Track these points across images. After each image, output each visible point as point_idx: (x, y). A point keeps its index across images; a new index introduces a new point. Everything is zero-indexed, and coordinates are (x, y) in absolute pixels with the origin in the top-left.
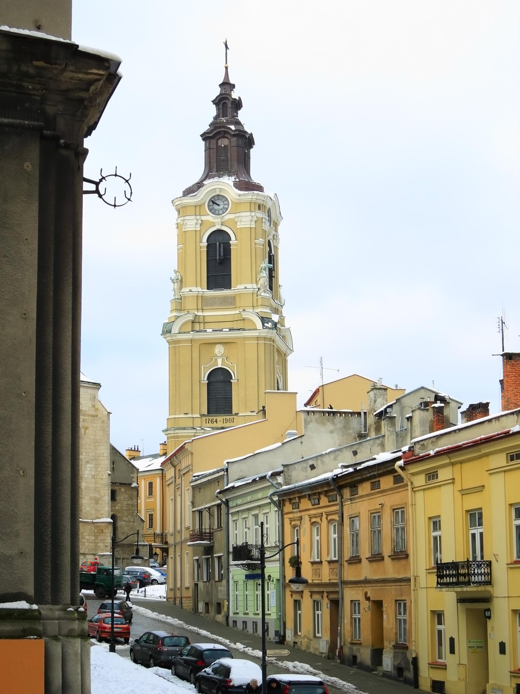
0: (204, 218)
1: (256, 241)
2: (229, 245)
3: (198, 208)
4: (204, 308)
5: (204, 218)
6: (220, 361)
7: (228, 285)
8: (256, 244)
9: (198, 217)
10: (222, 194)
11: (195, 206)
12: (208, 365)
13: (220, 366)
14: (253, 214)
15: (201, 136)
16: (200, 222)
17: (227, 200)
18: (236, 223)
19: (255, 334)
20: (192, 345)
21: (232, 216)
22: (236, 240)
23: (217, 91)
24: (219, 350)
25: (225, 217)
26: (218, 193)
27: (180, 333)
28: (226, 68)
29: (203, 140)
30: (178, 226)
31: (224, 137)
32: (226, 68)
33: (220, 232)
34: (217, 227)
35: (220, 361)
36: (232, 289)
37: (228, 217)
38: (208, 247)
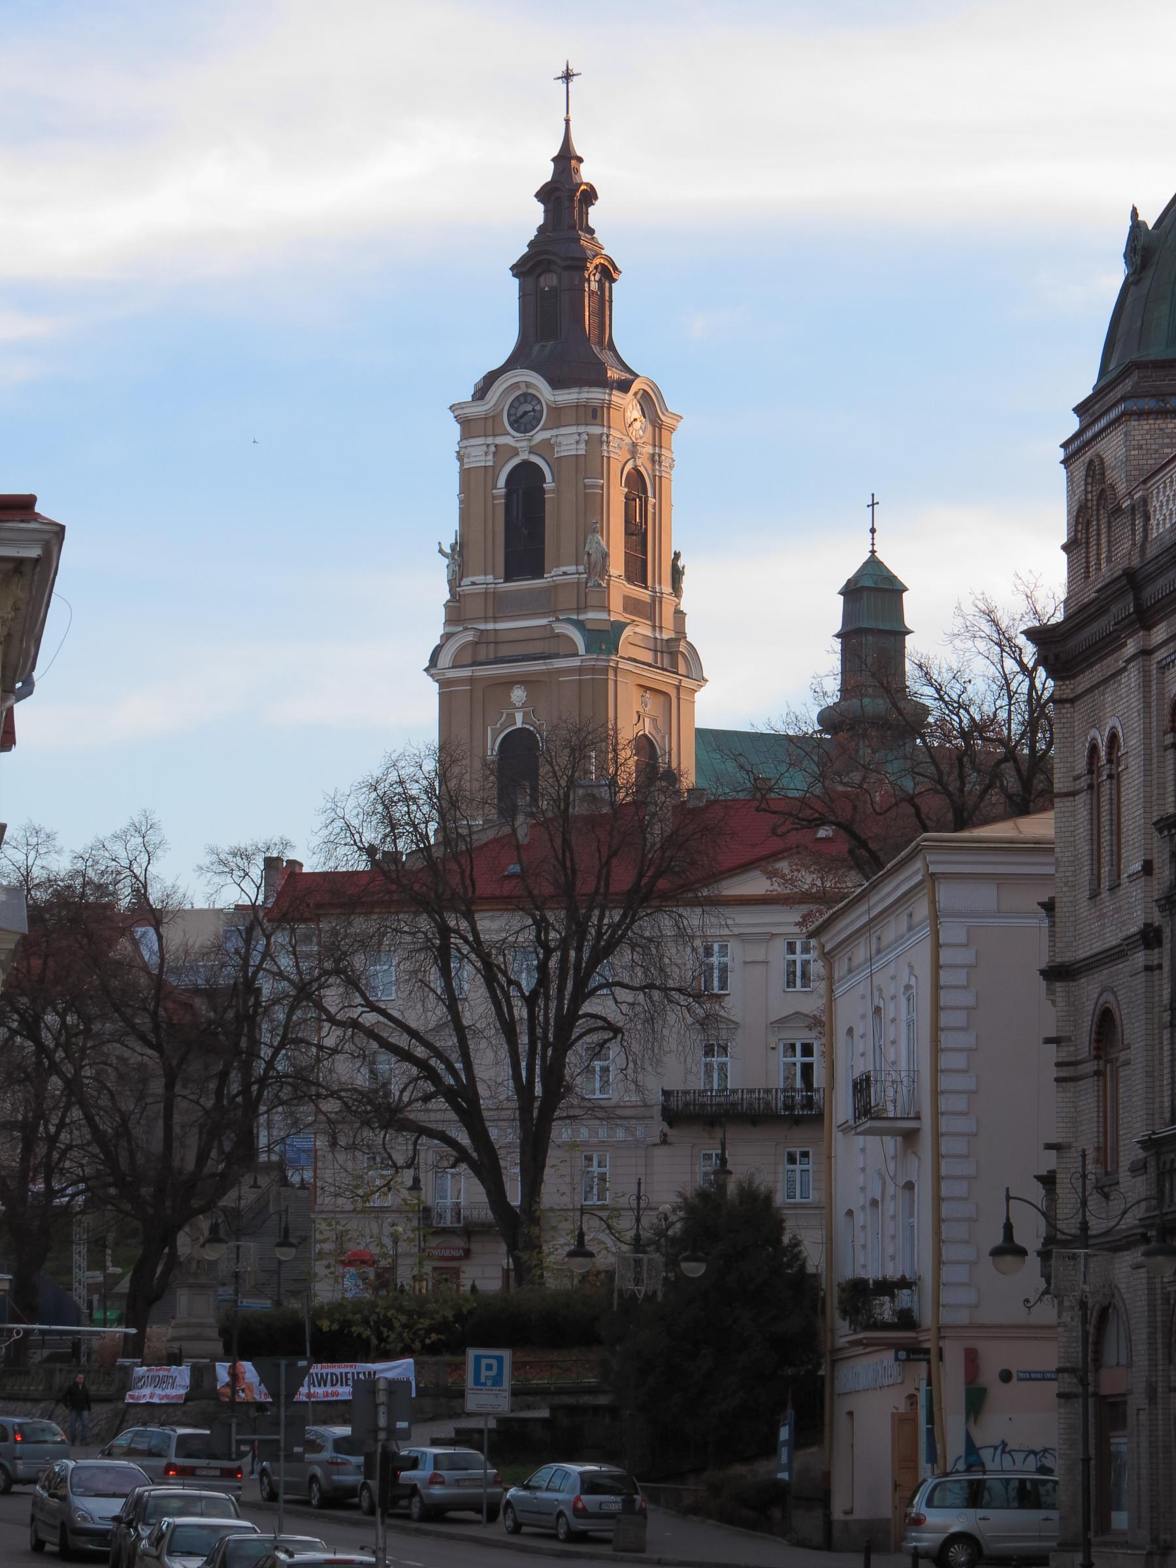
0: (501, 440)
1: (586, 480)
2: (543, 491)
3: (490, 423)
4: (497, 615)
5: (501, 440)
6: (519, 717)
7: (538, 573)
8: (586, 487)
9: (490, 440)
10: (531, 391)
11: (485, 418)
12: (498, 725)
13: (519, 725)
14: (582, 429)
15: (512, 269)
16: (492, 449)
17: (539, 402)
18: (552, 447)
19: (575, 662)
20: (471, 690)
21: (546, 435)
22: (554, 481)
23: (546, 173)
24: (518, 695)
25: (536, 437)
26: (523, 389)
27: (453, 667)
28: (567, 121)
29: (514, 275)
30: (460, 457)
31: (549, 271)
32: (567, 121)
33: (526, 466)
34: (524, 456)
35: (519, 717)
36: (545, 576)
37: (539, 435)
38: (508, 496)
